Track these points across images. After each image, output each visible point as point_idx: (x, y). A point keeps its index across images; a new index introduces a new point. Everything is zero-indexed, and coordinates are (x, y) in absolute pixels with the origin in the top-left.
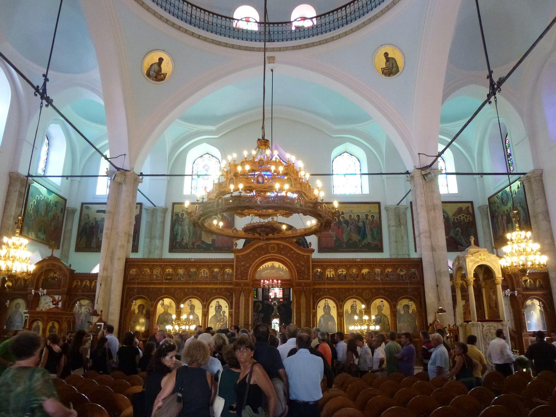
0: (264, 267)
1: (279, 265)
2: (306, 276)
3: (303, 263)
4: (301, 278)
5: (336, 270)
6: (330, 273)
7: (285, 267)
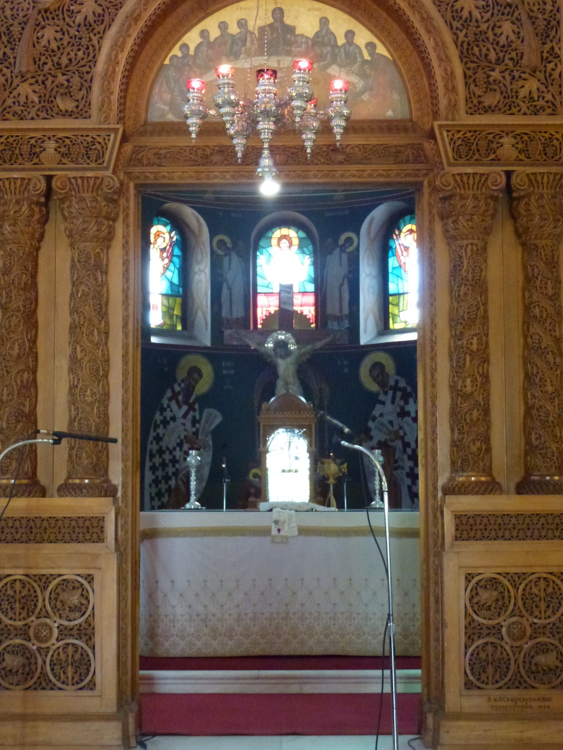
0: (215, 33)
1: (324, 22)
4: (490, 100)
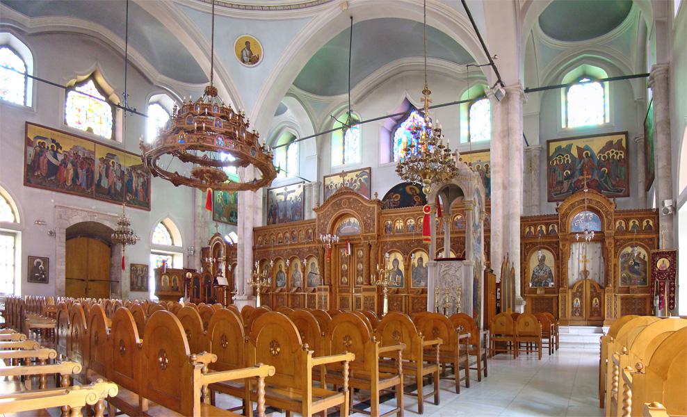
3: (369, 216)
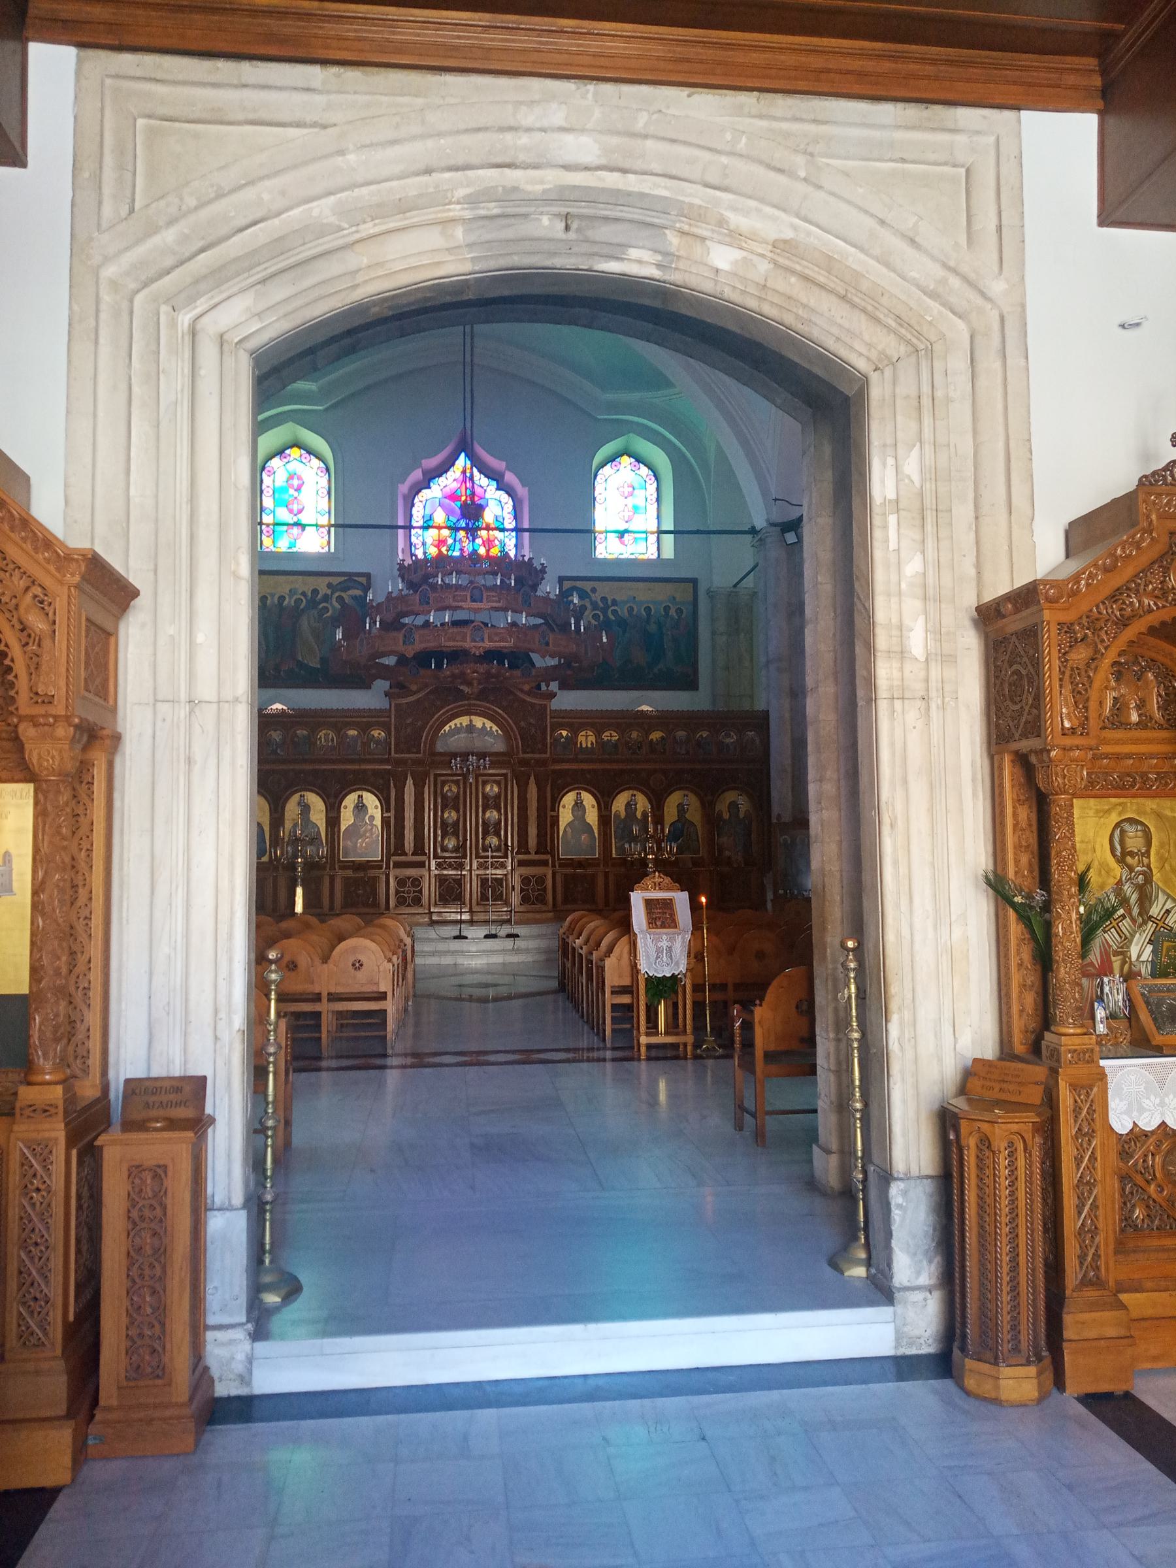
0: (453, 727)
1: (484, 724)
2: (540, 746)
5: (598, 735)
6: (587, 739)
7: (495, 728)
